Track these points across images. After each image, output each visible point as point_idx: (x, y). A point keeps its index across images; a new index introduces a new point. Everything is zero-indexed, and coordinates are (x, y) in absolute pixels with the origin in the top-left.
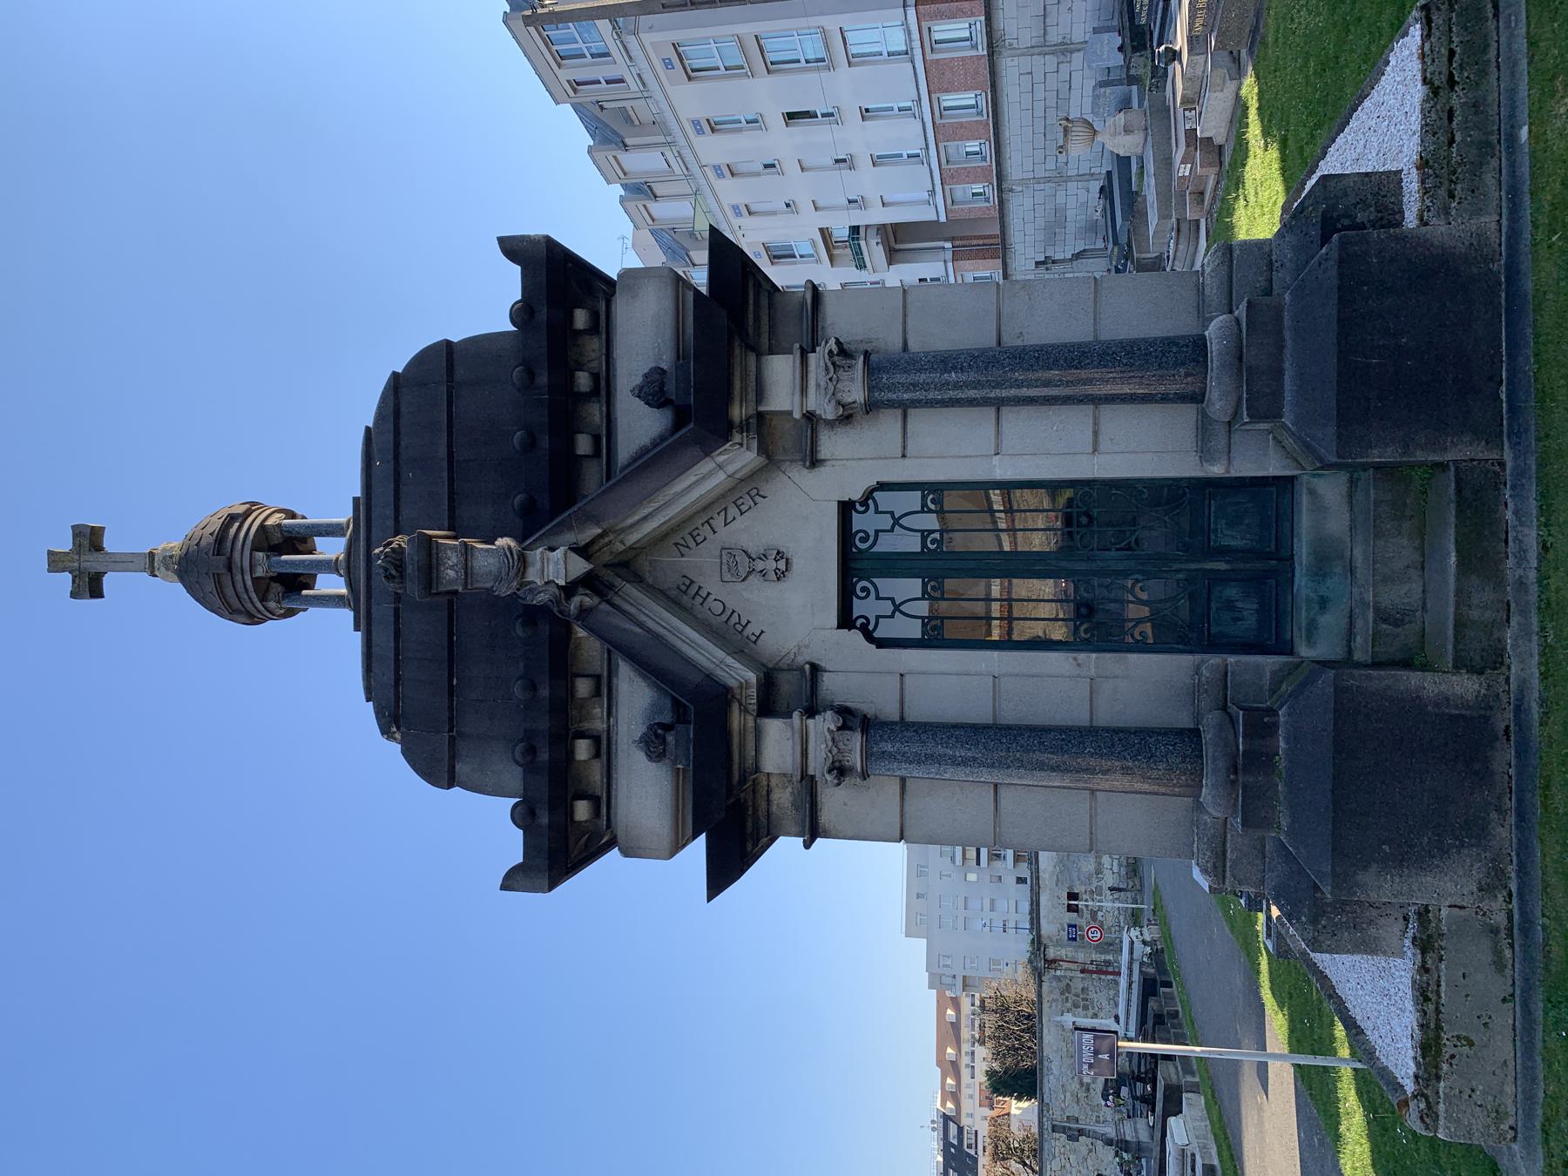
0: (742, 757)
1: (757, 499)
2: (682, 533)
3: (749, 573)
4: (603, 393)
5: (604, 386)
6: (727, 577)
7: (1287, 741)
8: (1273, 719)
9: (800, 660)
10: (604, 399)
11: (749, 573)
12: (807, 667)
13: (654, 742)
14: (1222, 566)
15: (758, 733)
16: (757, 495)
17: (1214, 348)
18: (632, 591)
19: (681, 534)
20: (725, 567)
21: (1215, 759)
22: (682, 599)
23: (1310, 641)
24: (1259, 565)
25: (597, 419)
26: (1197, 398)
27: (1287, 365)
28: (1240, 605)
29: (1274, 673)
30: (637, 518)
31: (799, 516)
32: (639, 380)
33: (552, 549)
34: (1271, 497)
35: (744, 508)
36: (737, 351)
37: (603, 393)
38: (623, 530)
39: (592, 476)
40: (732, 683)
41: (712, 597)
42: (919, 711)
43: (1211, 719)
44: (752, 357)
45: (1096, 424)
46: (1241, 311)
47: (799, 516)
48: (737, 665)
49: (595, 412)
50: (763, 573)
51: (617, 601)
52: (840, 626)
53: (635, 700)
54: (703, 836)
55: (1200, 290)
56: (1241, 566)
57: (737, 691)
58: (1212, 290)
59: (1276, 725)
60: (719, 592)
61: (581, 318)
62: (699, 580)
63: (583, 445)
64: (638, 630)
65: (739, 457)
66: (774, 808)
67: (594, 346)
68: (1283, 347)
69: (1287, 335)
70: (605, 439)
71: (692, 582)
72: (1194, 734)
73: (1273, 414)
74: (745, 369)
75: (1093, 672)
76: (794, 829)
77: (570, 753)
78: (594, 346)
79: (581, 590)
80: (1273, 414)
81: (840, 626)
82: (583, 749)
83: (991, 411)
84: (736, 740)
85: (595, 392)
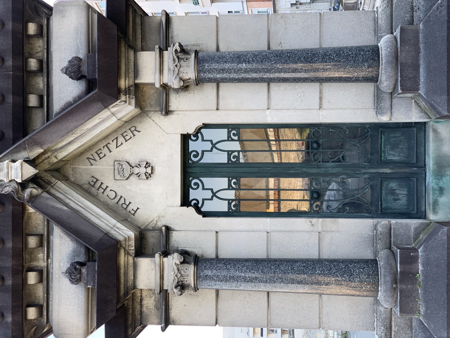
0: (126, 281)
1: (135, 133)
2: (91, 152)
3: (130, 175)
4: (45, 70)
5: (45, 67)
6: (118, 177)
7: (423, 266)
8: (415, 254)
9: (160, 224)
10: (45, 75)
11: (130, 175)
12: (164, 228)
13: (75, 273)
14: (388, 171)
15: (135, 266)
16: (135, 131)
17: (383, 52)
18: (61, 185)
19: (91, 152)
20: (116, 172)
21: (385, 276)
22: (91, 190)
23: (435, 211)
24: (407, 170)
25: (41, 86)
26: (374, 79)
27: (421, 62)
28: (397, 192)
29: (416, 229)
30: (64, 143)
31: (158, 143)
32: (66, 64)
33: (14, 161)
34: (414, 133)
35: (127, 138)
36: (123, 49)
37: (45, 70)
38: (56, 150)
39: (38, 119)
40: (120, 238)
41: (109, 189)
42: (226, 252)
43: (383, 255)
44: (132, 53)
45: (321, 93)
46: (397, 33)
47: (158, 143)
48: (123, 227)
49: (40, 82)
50: (138, 175)
51: (53, 191)
52: (182, 205)
53: (63, 249)
55: (376, 20)
56: (398, 170)
57: (123, 243)
58: (383, 22)
59: (417, 257)
60: (114, 186)
61: (32, 28)
62: (101, 179)
63: (33, 101)
64: (65, 208)
65: (124, 109)
66: (144, 309)
67: (40, 44)
68: (419, 52)
69: (422, 46)
70: (46, 98)
71: (97, 180)
72: (374, 262)
73: (415, 89)
74: (127, 59)
75: (320, 229)
76: (157, 321)
77: (25, 280)
78: (40, 44)
79: (31, 185)
80: (415, 89)
81: (182, 205)
82: (32, 278)
83: (265, 85)
84: (122, 271)
85: (41, 70)
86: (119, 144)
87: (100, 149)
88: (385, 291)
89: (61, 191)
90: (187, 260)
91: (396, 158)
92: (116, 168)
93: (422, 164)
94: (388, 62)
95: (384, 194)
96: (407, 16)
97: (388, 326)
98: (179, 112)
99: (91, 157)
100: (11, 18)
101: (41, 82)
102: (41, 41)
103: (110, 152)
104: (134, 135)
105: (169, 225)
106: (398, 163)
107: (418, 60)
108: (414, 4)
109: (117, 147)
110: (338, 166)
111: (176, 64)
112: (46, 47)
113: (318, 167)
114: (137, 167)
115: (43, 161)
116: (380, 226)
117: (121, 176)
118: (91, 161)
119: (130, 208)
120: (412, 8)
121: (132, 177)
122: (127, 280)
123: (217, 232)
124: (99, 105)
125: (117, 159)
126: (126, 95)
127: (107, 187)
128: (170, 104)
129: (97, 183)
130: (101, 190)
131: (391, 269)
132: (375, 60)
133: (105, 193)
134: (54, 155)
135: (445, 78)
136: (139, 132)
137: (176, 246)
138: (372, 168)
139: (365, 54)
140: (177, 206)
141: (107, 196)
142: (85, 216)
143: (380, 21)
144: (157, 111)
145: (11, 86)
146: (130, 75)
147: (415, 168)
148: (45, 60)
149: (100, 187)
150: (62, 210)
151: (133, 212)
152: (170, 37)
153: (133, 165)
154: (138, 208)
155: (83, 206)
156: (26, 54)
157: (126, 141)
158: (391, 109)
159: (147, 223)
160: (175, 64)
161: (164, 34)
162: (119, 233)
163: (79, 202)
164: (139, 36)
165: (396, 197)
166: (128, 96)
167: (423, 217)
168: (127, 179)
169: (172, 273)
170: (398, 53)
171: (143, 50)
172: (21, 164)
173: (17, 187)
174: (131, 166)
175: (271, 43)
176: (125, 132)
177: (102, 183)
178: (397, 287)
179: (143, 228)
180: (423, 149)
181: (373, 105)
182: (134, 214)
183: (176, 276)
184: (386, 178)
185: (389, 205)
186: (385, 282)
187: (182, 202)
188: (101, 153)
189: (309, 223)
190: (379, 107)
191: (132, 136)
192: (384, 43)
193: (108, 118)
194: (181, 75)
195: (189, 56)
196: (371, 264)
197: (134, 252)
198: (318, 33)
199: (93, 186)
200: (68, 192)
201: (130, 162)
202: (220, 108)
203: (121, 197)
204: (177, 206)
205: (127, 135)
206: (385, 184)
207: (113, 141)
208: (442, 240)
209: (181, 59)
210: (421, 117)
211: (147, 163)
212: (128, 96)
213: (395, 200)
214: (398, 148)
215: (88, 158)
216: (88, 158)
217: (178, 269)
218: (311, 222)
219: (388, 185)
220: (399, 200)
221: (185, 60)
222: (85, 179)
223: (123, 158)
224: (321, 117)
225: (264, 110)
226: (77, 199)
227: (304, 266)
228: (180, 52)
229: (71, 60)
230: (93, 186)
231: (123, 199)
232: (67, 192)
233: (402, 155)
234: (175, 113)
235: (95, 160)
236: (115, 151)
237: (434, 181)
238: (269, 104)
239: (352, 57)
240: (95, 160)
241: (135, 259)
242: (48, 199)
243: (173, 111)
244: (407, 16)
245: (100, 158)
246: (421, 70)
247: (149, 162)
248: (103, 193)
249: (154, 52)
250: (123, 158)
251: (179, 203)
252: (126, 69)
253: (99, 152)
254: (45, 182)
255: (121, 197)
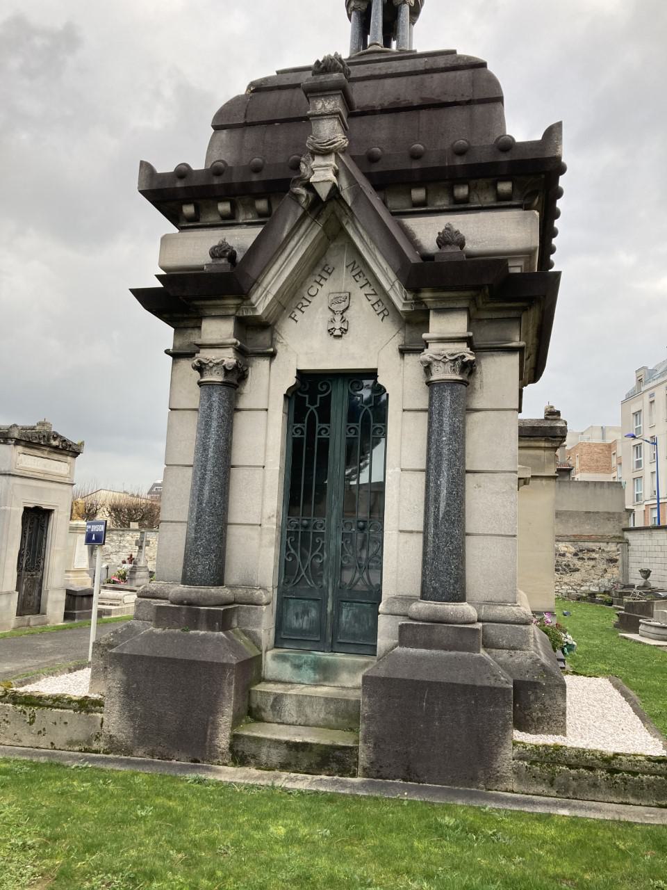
0: (209, 307)
1: (382, 315)
2: (361, 267)
3: (333, 311)
4: (456, 207)
5: (461, 206)
6: (332, 297)
7: (204, 635)
8: (217, 628)
9: (279, 347)
10: (451, 207)
11: (333, 311)
12: (272, 350)
13: (221, 252)
14: (329, 609)
15: (224, 317)
16: (384, 315)
17: (451, 608)
18: (316, 231)
19: (361, 265)
20: (338, 295)
21: (197, 592)
22: (315, 266)
23: (276, 657)
24: (329, 631)
25: (439, 203)
26: (424, 596)
27: (434, 651)
28: (306, 618)
29: (255, 633)
30: (361, 230)
31: (368, 344)
32: (456, 228)
33: (336, 174)
34: (365, 642)
35: (376, 306)
36: (468, 294)
37: (456, 207)
38: (354, 222)
39: (398, 203)
40: (253, 299)
41: (319, 287)
42: (241, 420)
43: (224, 592)
44: (464, 304)
45: (418, 532)
46: (479, 626)
47: (368, 344)
48: (267, 302)
49: (442, 203)
50: (333, 321)
51: (308, 221)
52: (299, 371)
53: (242, 238)
54: (161, 285)
55: (503, 603)
56: (329, 620)
57: (248, 302)
58: (499, 611)
59: (213, 630)
60: (322, 294)
61: (505, 187)
62: (331, 279)
63: (418, 194)
64: (285, 234)
65: (399, 298)
66: (189, 331)
67: (489, 199)
68: (446, 650)
69: (453, 653)
70: (422, 209)
71: (330, 274)
72: (219, 581)
73: (402, 643)
74: (457, 299)
75: (265, 526)
76: (177, 344)
77: (222, 199)
78: (489, 199)
79: (311, 195)
80: (402, 643)
81: (299, 371)
82: (224, 207)
83: (424, 467)
84: (219, 302)
85: (456, 201)
86: (369, 297)
87: (364, 276)
88: (182, 591)
89: (309, 230)
90: (230, 375)
91: (343, 618)
92: (342, 295)
93: (336, 648)
94: (436, 610)
95: (303, 602)
96: (504, 642)
97: (156, 595)
98: (402, 365)
99: (356, 266)
100: (513, 159)
101: (443, 203)
102: (493, 199)
103: (361, 287)
104: (378, 314)
105: (277, 357)
106: (338, 620)
107: (437, 647)
108: (519, 652)
109: (366, 295)
110: (337, 551)
111: (447, 357)
112: (485, 205)
113: (338, 527)
114: (343, 317)
115: (342, 207)
116: (261, 593)
117: (332, 300)
118: (352, 266)
119: (298, 312)
120: (514, 649)
121: (331, 313)
122: (209, 308)
123: (267, 410)
124: (398, 266)
125: (352, 296)
126: (413, 299)
127: (322, 285)
128: (411, 355)
129: (327, 274)
130: (318, 279)
131: (204, 599)
132: (442, 596)
133: (316, 283)
134: (349, 220)
135: (406, 676)
136: (382, 320)
137: (254, 364)
138: (333, 590)
139: (450, 585)
140: (297, 365)
141: (312, 286)
142: (278, 258)
143: (500, 608)
144: (404, 340)
145: (431, 165)
146: (439, 304)
147: (330, 641)
148: (469, 206)
149: (322, 278)
150: (283, 229)
151: (293, 316)
152: (493, 353)
153: (344, 314)
154: (297, 321)
155: (291, 256)
156: (473, 182)
157: (373, 305)
158: (392, 615)
159: (280, 332)
160: (447, 355)
161: (495, 346)
162: (260, 296)
163: (296, 252)
164: (495, 315)
165: (300, 616)
166: (413, 301)
167: (277, 646)
168: (329, 308)
169: (213, 357)
170: (446, 623)
171: (470, 320)
172: (329, 181)
173: (306, 178)
174: (344, 311)
175: (480, 474)
176: (383, 304)
177: (326, 279)
178: (184, 605)
179: (276, 327)
180: (353, 651)
181: (401, 594)
182: (290, 317)
183: (211, 362)
184: (322, 604)
185: (291, 607)
186: (190, 592)
187: (304, 372)
188: (360, 277)
189: (272, 514)
190: (395, 600)
191: (378, 312)
192: (466, 609)
193: (388, 279)
194: (435, 363)
195: (458, 373)
196: (214, 578)
197: (241, 315)
198: (490, 532)
199: (323, 270)
200: (308, 239)
201: (348, 311)
202: (406, 413)
203: (310, 302)
204: (297, 365)
205: (379, 306)
206: (314, 603)
207: (373, 290)
208: (223, 657)
209: (454, 363)
210: (380, 651)
211: (346, 330)
212: (413, 301)
213: (297, 615)
214: (355, 622)
215: (355, 262)
216: (355, 262)
217: (218, 364)
218: (273, 516)
219: (314, 607)
220: (297, 618)
221: (453, 368)
222: (332, 259)
223: (353, 302)
224: (390, 532)
225: (400, 464)
226: (300, 248)
227: (215, 504)
228: (462, 362)
229: (459, 233)
230: (323, 270)
231: (308, 303)
232: (309, 236)
233: (347, 626)
234: (402, 361)
235: (352, 270)
236: (362, 293)
237: (309, 659)
238: (407, 470)
239: (447, 569)
240: (352, 270)
241: (233, 317)
242: (296, 214)
243: (404, 359)
244: (504, 642)
245: (354, 276)
246: (423, 651)
247: (348, 333)
248: (316, 281)
249: (466, 330)
250: (353, 302)
251: (302, 367)
252: (444, 298)
253: (361, 275)
254: (319, 212)
255: (310, 302)
